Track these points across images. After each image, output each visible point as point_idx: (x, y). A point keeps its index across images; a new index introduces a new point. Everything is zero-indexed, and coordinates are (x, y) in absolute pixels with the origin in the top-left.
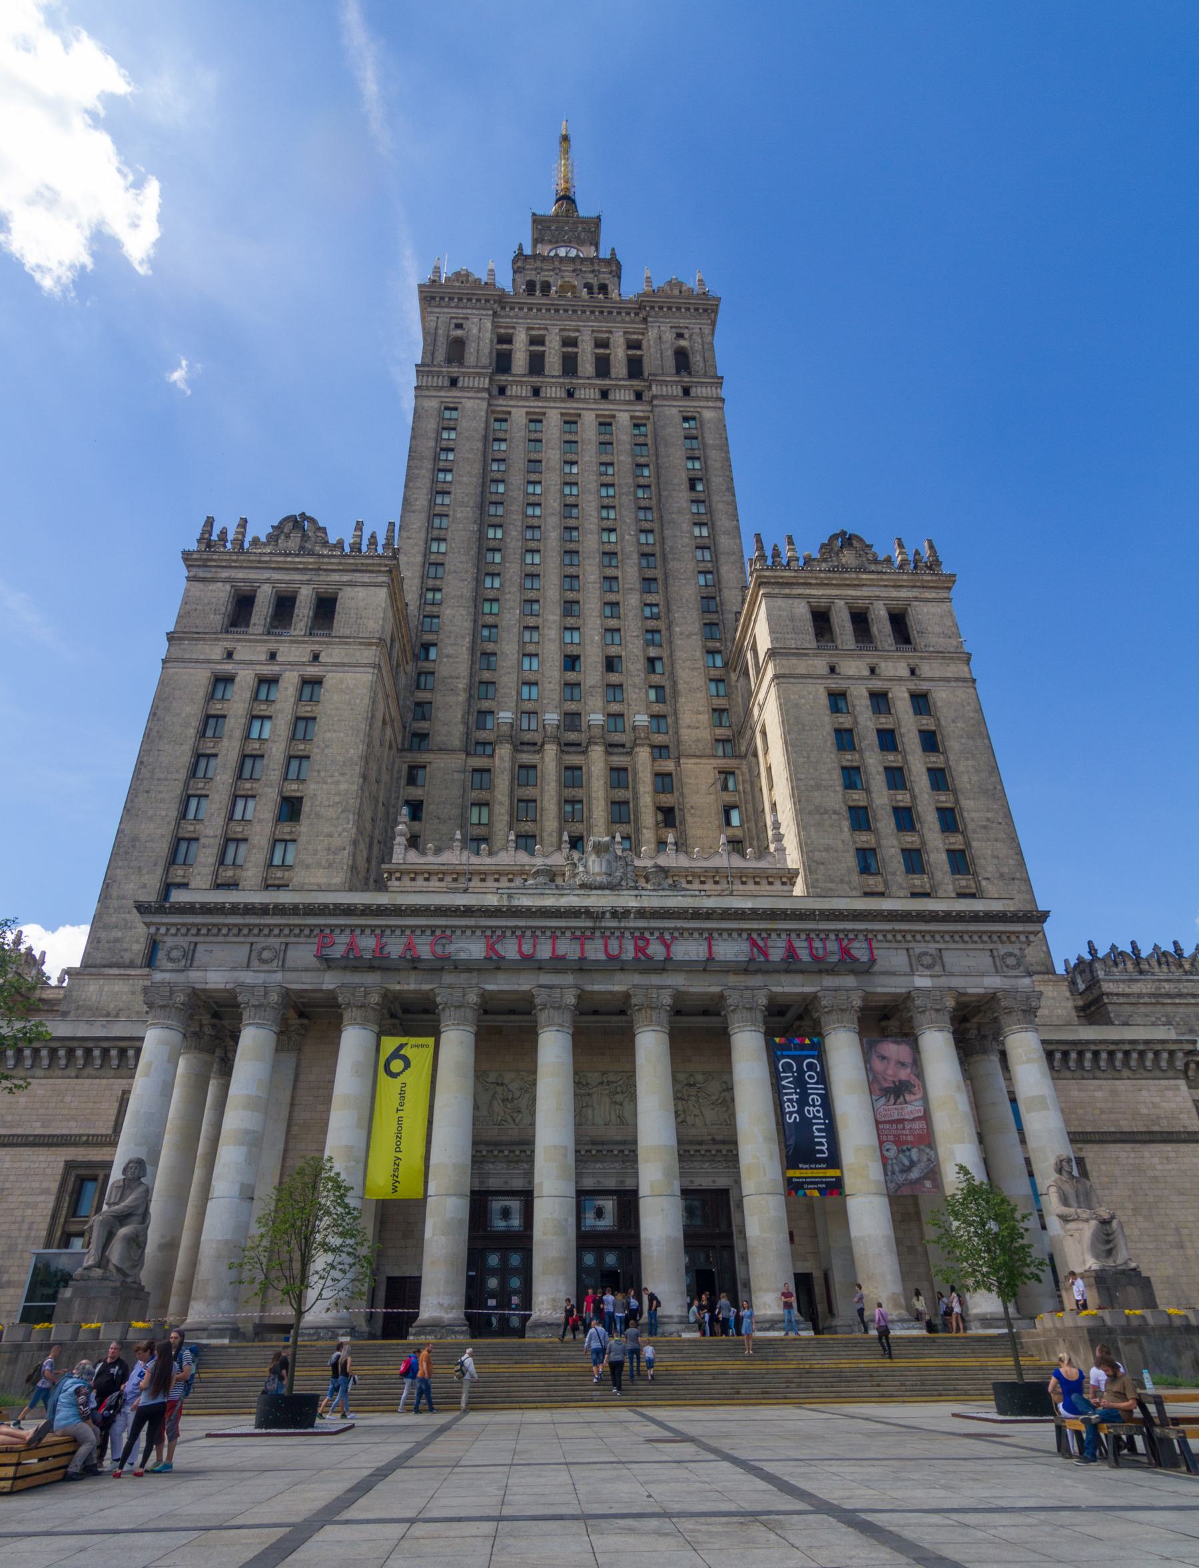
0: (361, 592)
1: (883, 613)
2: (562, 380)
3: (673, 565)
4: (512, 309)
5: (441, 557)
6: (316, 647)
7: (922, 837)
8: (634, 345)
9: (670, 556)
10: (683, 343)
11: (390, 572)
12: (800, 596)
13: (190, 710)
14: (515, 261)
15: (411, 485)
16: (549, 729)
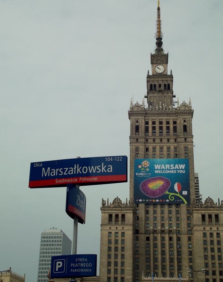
0: (128, 214)
2: (159, 137)
4: (148, 114)
6: (123, 226)
7: (215, 261)
8: (175, 123)
10: (185, 124)
11: (133, 210)
12: (200, 213)
13: (106, 239)
14: (147, 78)
15: (131, 171)
16: (159, 230)
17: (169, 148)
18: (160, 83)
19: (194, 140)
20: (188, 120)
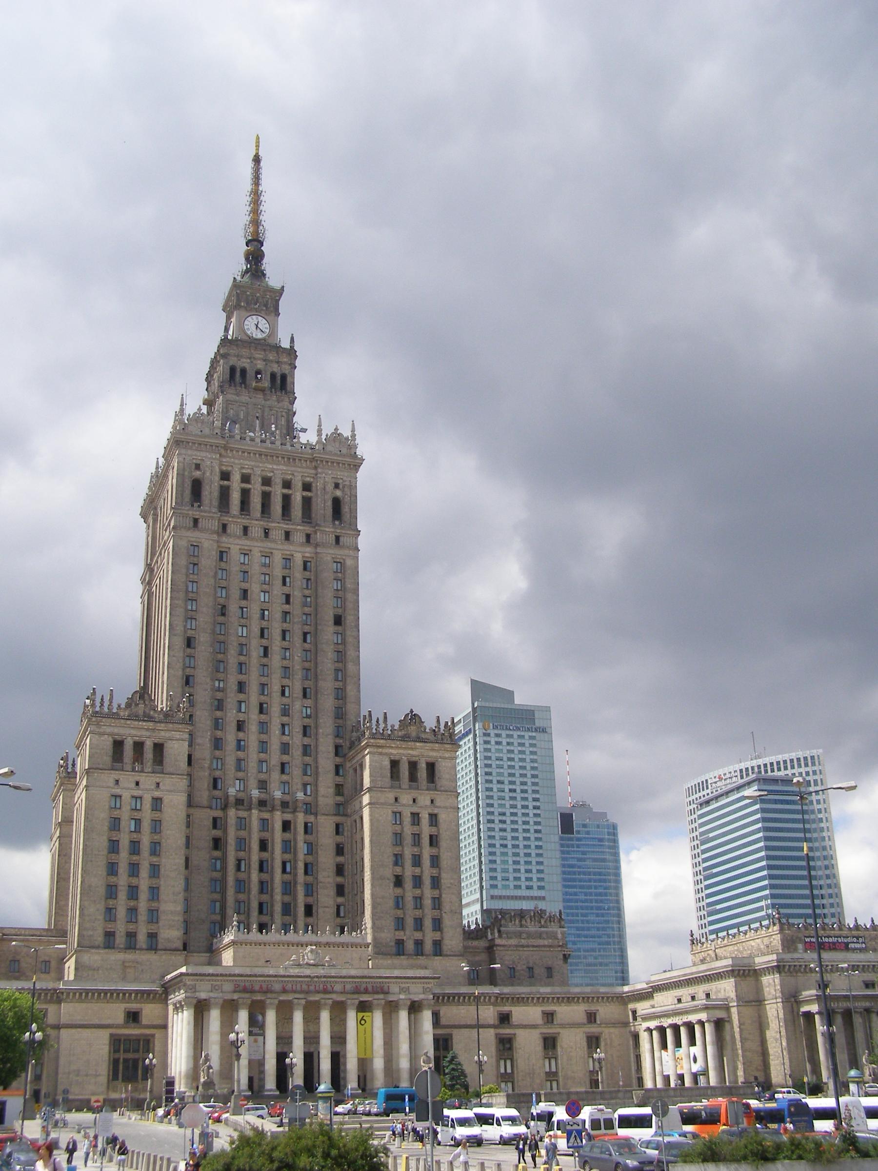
1: (424, 765)
2: (262, 523)
3: (321, 683)
5: (192, 670)
6: (158, 780)
7: (422, 891)
8: (307, 487)
9: (320, 677)
10: (338, 493)
12: (386, 754)
15: (173, 613)
16: (254, 799)
17: (288, 560)
18: (259, 366)
19: (362, 542)
20: (347, 483)
